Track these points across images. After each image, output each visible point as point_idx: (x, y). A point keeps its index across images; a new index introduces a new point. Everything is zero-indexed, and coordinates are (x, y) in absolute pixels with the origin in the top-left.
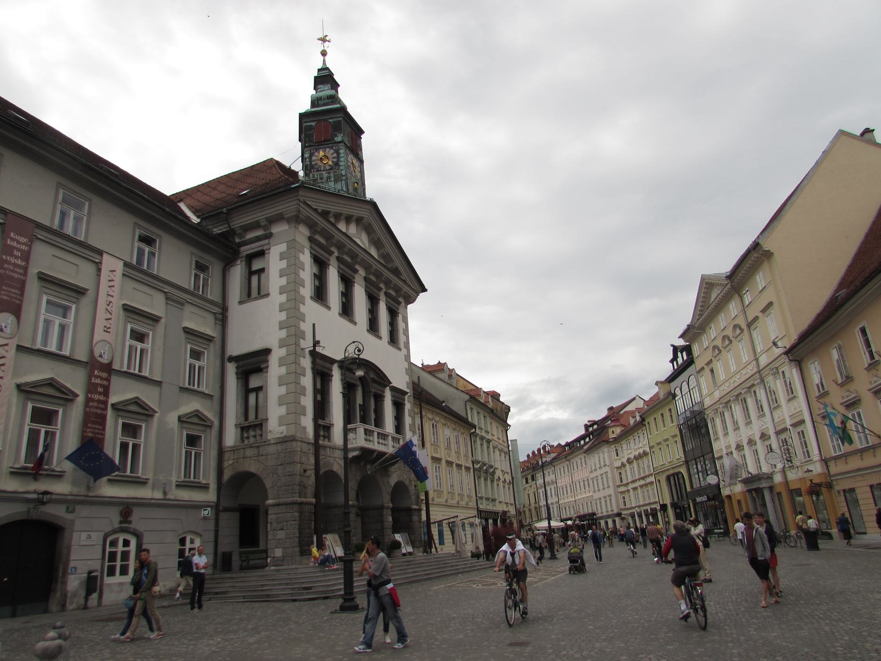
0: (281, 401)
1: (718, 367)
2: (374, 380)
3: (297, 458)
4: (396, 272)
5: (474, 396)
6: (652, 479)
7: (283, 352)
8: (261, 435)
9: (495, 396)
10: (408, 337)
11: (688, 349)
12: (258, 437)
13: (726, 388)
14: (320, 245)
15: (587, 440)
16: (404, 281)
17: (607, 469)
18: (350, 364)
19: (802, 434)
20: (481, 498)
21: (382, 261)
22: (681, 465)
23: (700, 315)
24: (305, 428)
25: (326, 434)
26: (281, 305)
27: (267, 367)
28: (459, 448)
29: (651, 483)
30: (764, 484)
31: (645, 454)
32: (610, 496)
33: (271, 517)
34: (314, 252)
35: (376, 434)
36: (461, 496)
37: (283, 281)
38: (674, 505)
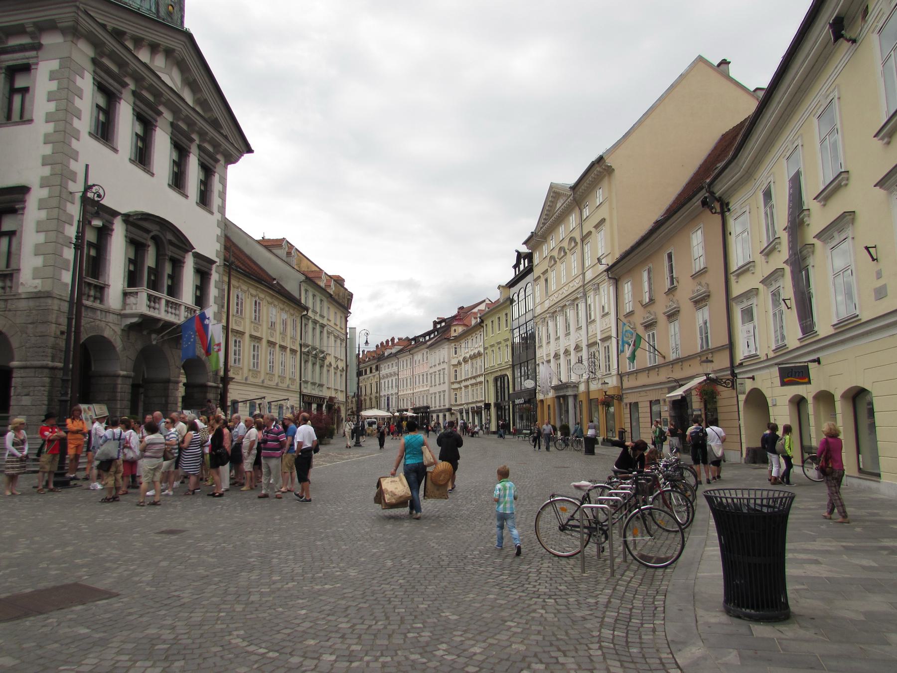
0: (38, 251)
1: (552, 276)
2: (171, 243)
3: (53, 317)
4: (215, 124)
5: (313, 278)
6: (482, 379)
7: (44, 193)
8: (11, 287)
9: (339, 281)
10: (224, 201)
11: (529, 257)
12: (8, 289)
13: (555, 299)
14: (108, 72)
15: (432, 336)
16: (226, 137)
17: (445, 366)
18: (141, 219)
19: (607, 349)
20: (306, 382)
21: (198, 109)
23: (544, 224)
24: (67, 284)
25: (98, 295)
26: (46, 136)
27: (24, 208)
28: (285, 329)
29: (481, 383)
30: (570, 392)
31: (479, 354)
32: (444, 391)
33: (16, 380)
34: (99, 79)
35: (163, 302)
36: (282, 378)
37: (52, 107)
38: (498, 406)
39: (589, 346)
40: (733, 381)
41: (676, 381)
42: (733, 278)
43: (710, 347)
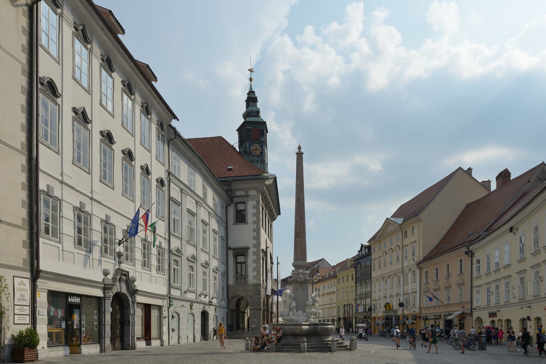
7: (255, 250)
11: (369, 248)
31: (334, 292)
42: (474, 280)
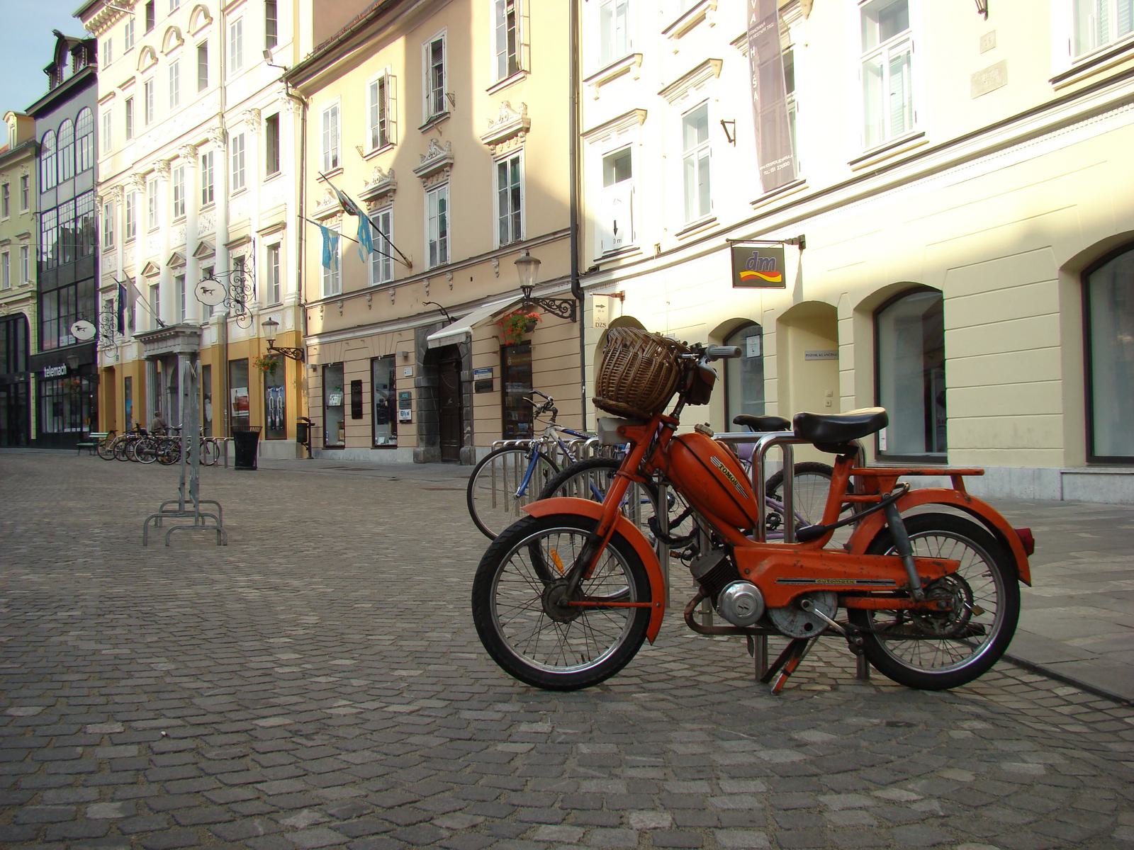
22: (26, 299)
39: (230, 246)
40: (574, 308)
41: (443, 311)
42: (586, 90)
43: (523, 238)
